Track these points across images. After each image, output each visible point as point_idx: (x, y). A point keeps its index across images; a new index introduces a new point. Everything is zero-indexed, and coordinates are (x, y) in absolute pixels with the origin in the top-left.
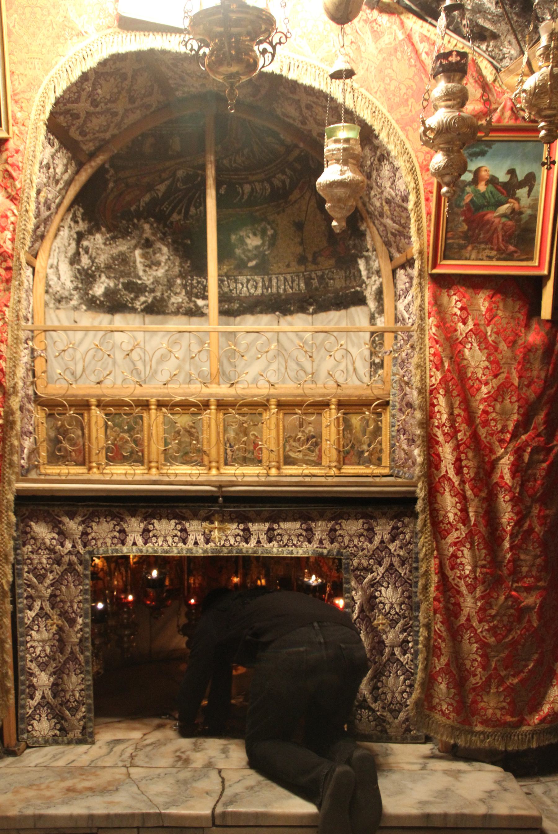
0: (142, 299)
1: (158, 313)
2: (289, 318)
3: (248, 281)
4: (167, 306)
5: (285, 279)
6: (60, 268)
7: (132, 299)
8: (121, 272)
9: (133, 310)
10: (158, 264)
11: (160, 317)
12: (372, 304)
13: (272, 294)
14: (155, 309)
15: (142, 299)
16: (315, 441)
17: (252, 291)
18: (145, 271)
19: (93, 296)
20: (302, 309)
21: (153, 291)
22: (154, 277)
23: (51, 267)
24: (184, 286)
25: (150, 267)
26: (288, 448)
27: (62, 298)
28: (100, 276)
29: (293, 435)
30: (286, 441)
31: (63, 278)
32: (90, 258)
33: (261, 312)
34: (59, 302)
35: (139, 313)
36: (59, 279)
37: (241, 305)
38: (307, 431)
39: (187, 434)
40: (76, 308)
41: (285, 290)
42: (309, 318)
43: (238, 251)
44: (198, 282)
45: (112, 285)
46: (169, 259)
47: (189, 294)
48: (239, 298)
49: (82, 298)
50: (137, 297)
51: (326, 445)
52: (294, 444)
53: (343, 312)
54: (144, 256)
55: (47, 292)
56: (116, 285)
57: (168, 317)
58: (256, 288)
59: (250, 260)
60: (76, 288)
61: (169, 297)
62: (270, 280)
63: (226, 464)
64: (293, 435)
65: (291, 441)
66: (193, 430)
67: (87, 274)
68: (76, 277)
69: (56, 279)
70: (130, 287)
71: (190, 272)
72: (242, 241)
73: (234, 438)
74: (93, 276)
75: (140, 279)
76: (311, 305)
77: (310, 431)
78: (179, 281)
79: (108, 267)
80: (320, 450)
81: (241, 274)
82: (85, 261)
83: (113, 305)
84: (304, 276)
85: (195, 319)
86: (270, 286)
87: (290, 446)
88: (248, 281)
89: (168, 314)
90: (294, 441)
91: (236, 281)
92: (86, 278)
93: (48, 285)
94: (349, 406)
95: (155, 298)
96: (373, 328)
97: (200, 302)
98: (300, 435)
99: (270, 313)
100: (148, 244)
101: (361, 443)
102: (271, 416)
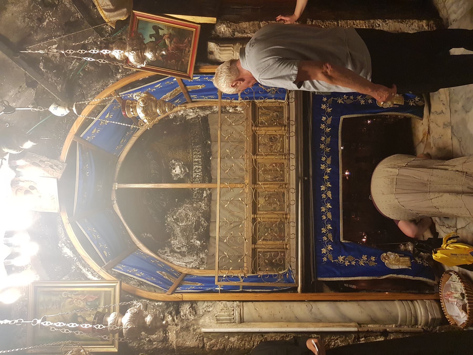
0: (203, 222)
1: (210, 216)
2: (213, 153)
3: (195, 172)
4: (206, 211)
5: (195, 155)
6: (187, 261)
7: (202, 227)
8: (189, 232)
9: (208, 226)
10: (186, 215)
11: (212, 214)
12: (208, 112)
13: (202, 161)
14: (208, 216)
15: (203, 222)
16: (272, 139)
17: (200, 170)
18: (189, 221)
19: (201, 246)
20: (209, 146)
21: (199, 217)
22: (192, 216)
23: (186, 266)
24: (197, 202)
25: (188, 218)
26: (276, 151)
27: (201, 261)
28: (191, 242)
29: (269, 148)
31: (192, 260)
32: (182, 247)
33: (210, 166)
34: (203, 262)
35: (209, 224)
36: (192, 262)
37: (207, 176)
40: (206, 254)
41: (200, 155)
42: (213, 143)
43: (182, 177)
44: (195, 196)
45: (195, 237)
46: (184, 209)
47: (201, 200)
48: (203, 177)
49: (202, 251)
50: (202, 225)
52: (274, 148)
53: (210, 127)
54: (182, 222)
55: (198, 268)
56: (196, 235)
57: (212, 209)
58: (199, 168)
59: (185, 171)
60: (197, 254)
61: (202, 210)
62: (195, 162)
63: (284, 181)
64: (269, 148)
67: (190, 249)
68: (192, 254)
69: (192, 264)
70: (197, 229)
71: (190, 199)
72: (177, 175)
74: (191, 246)
75: (193, 223)
76: (207, 142)
78: (195, 205)
79: (188, 238)
81: (192, 176)
82: (184, 249)
83: (206, 236)
84: (194, 146)
85: (213, 198)
86: (198, 162)
88: (195, 172)
89: (210, 210)
91: (195, 178)
92: (192, 250)
93: (195, 268)
94: (255, 122)
95: (202, 217)
96: (220, 112)
97: (205, 195)
99: (210, 162)
100: (177, 220)
102: (260, 159)
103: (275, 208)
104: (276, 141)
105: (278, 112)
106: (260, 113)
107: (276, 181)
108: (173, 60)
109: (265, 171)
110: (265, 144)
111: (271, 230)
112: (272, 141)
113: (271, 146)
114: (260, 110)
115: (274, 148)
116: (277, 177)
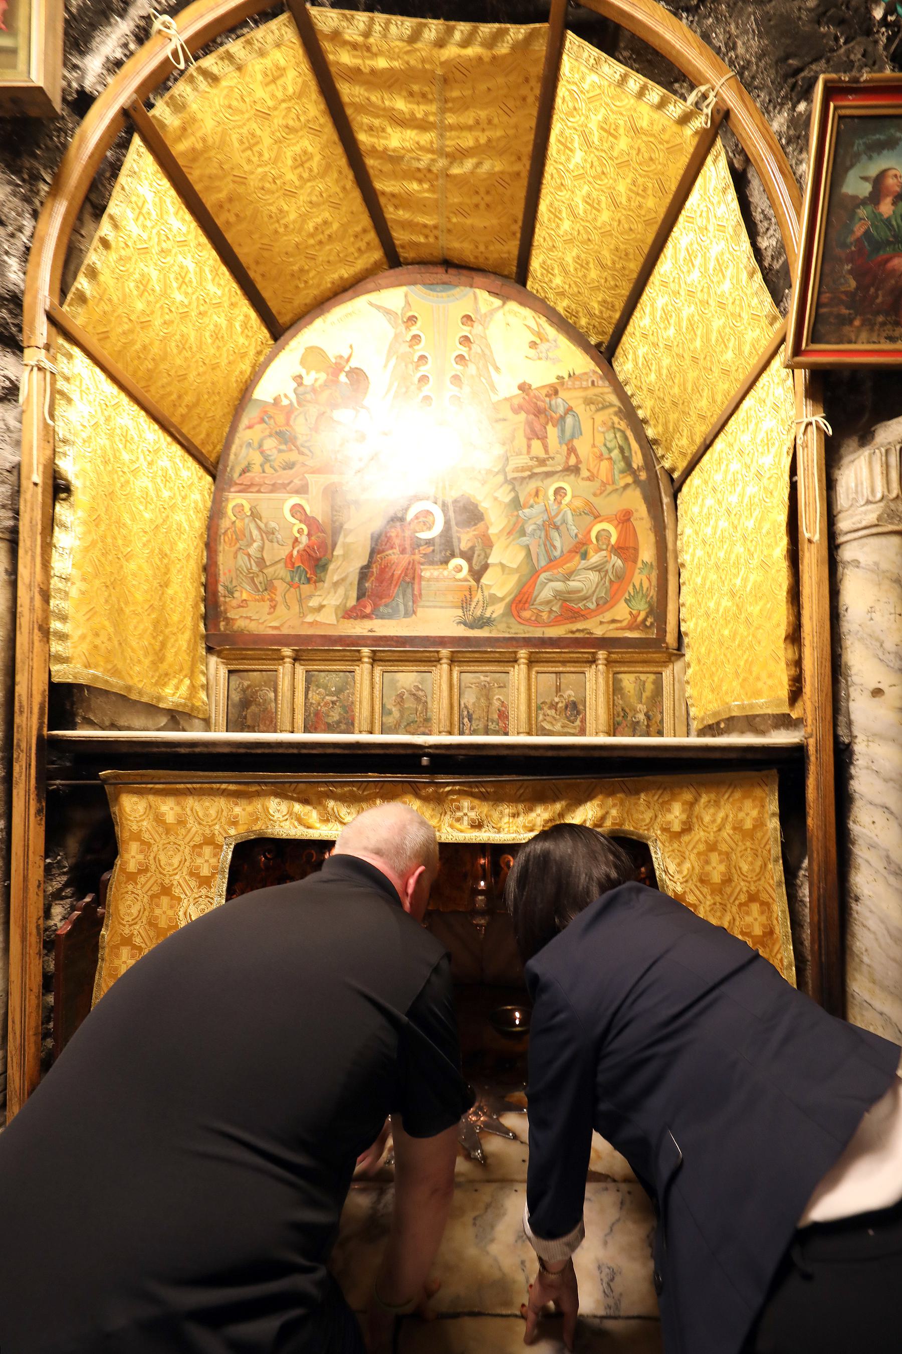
26: (541, 717)
29: (548, 701)
30: (539, 708)
38: (565, 696)
39: (412, 699)
51: (590, 715)
52: (549, 712)
64: (548, 701)
65: (545, 708)
66: (421, 693)
73: (474, 704)
77: (569, 696)
80: (583, 721)
87: (544, 715)
90: (550, 708)
98: (557, 699)
101: (636, 711)
103: (390, 713)
104: (567, 717)
105: (648, 726)
106: (643, 677)
107: (461, 717)
108: (853, 284)
109: (486, 692)
110: (558, 689)
111: (333, 703)
112: (566, 707)
113: (553, 706)
114: (652, 677)
115: (549, 712)
116: (470, 720)
